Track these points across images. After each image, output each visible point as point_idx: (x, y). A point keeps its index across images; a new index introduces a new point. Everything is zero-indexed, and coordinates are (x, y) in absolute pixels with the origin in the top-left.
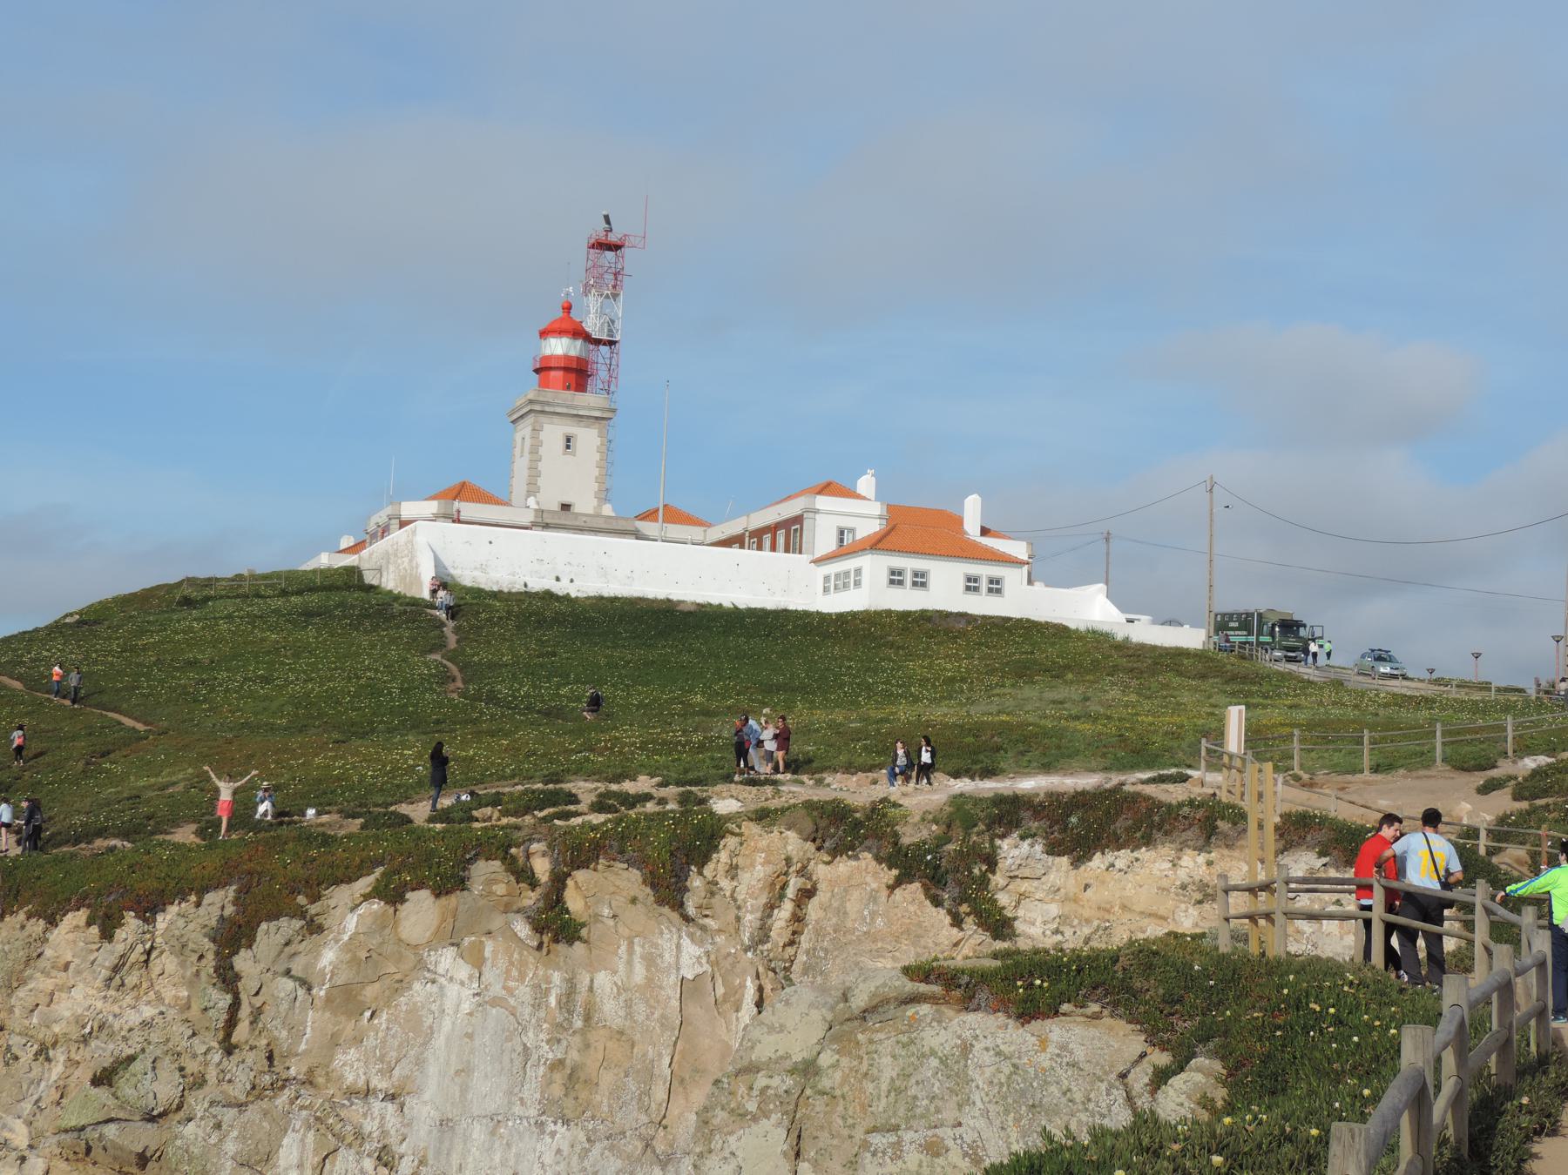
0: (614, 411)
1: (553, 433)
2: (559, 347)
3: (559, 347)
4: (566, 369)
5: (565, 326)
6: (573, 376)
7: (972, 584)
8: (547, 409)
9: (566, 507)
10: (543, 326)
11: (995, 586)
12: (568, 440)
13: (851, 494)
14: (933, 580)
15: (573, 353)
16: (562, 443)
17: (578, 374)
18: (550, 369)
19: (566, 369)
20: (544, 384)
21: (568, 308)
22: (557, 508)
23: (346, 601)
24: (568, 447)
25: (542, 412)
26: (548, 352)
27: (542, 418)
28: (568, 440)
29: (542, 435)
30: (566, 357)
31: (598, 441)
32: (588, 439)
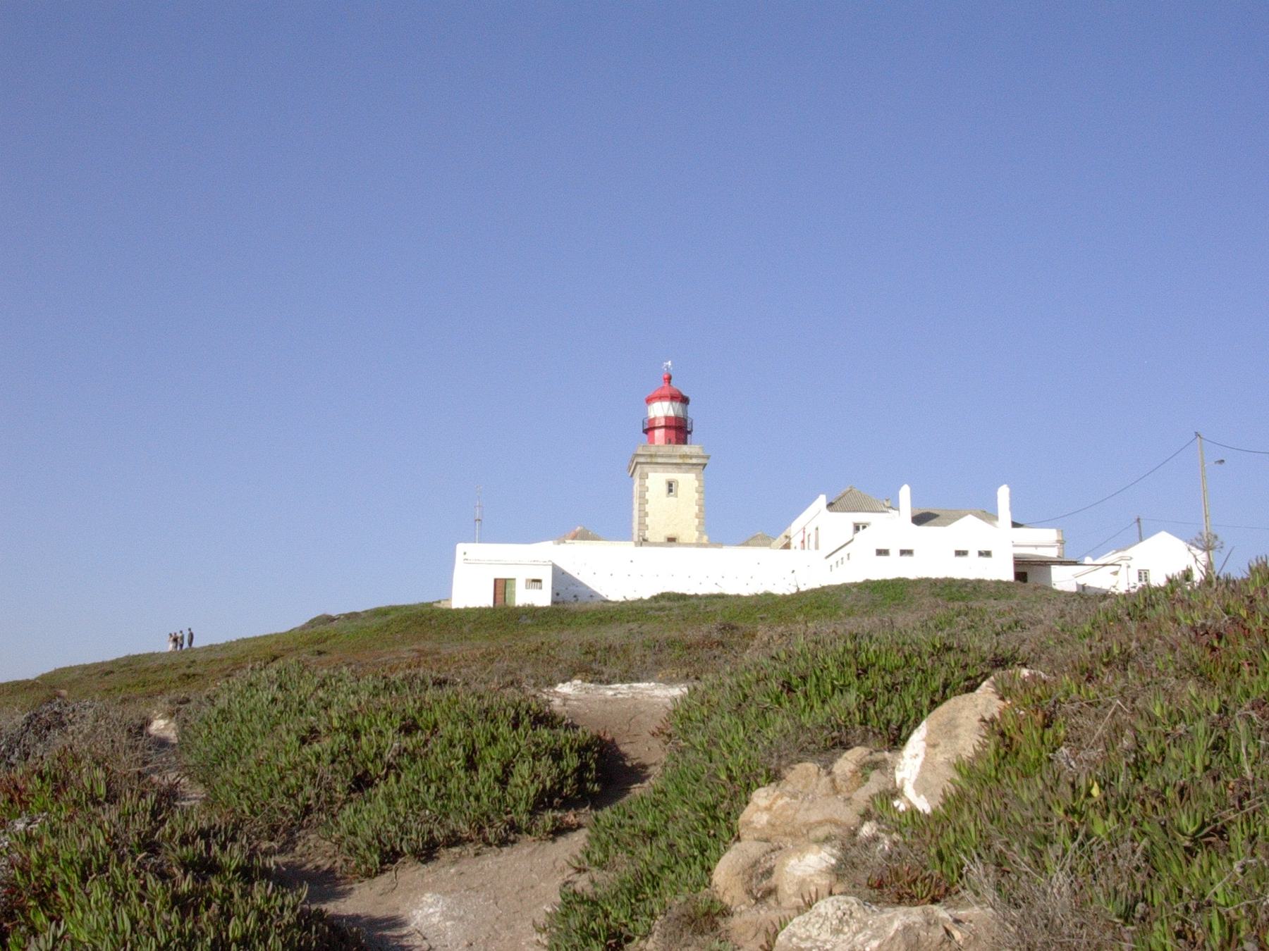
0: (708, 457)
1: (656, 480)
2: (662, 410)
4: (665, 427)
5: (666, 392)
6: (673, 432)
9: (671, 540)
10: (650, 393)
15: (671, 413)
16: (665, 488)
17: (679, 430)
18: (655, 428)
19: (665, 427)
23: (431, 621)
24: (670, 491)
26: (652, 415)
27: (647, 468)
28: (670, 485)
29: (648, 483)
30: (667, 418)
31: (696, 484)
32: (688, 482)
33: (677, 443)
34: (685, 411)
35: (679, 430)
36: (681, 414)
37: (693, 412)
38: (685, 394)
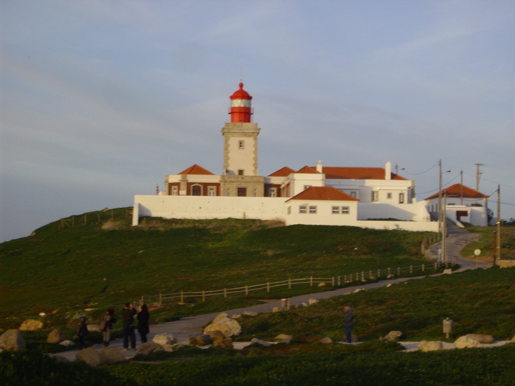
0: (259, 129)
2: (238, 103)
3: (238, 103)
4: (239, 112)
7: (335, 210)
8: (231, 131)
10: (231, 94)
11: (346, 210)
12: (241, 143)
13: (312, 170)
14: (318, 210)
15: (242, 106)
16: (237, 145)
20: (232, 121)
21: (241, 85)
22: (237, 173)
24: (241, 146)
25: (229, 132)
28: (241, 143)
29: (230, 142)
32: (249, 141)
33: (245, 122)
34: (250, 104)
35: (245, 115)
36: (247, 106)
37: (254, 105)
38: (251, 94)
